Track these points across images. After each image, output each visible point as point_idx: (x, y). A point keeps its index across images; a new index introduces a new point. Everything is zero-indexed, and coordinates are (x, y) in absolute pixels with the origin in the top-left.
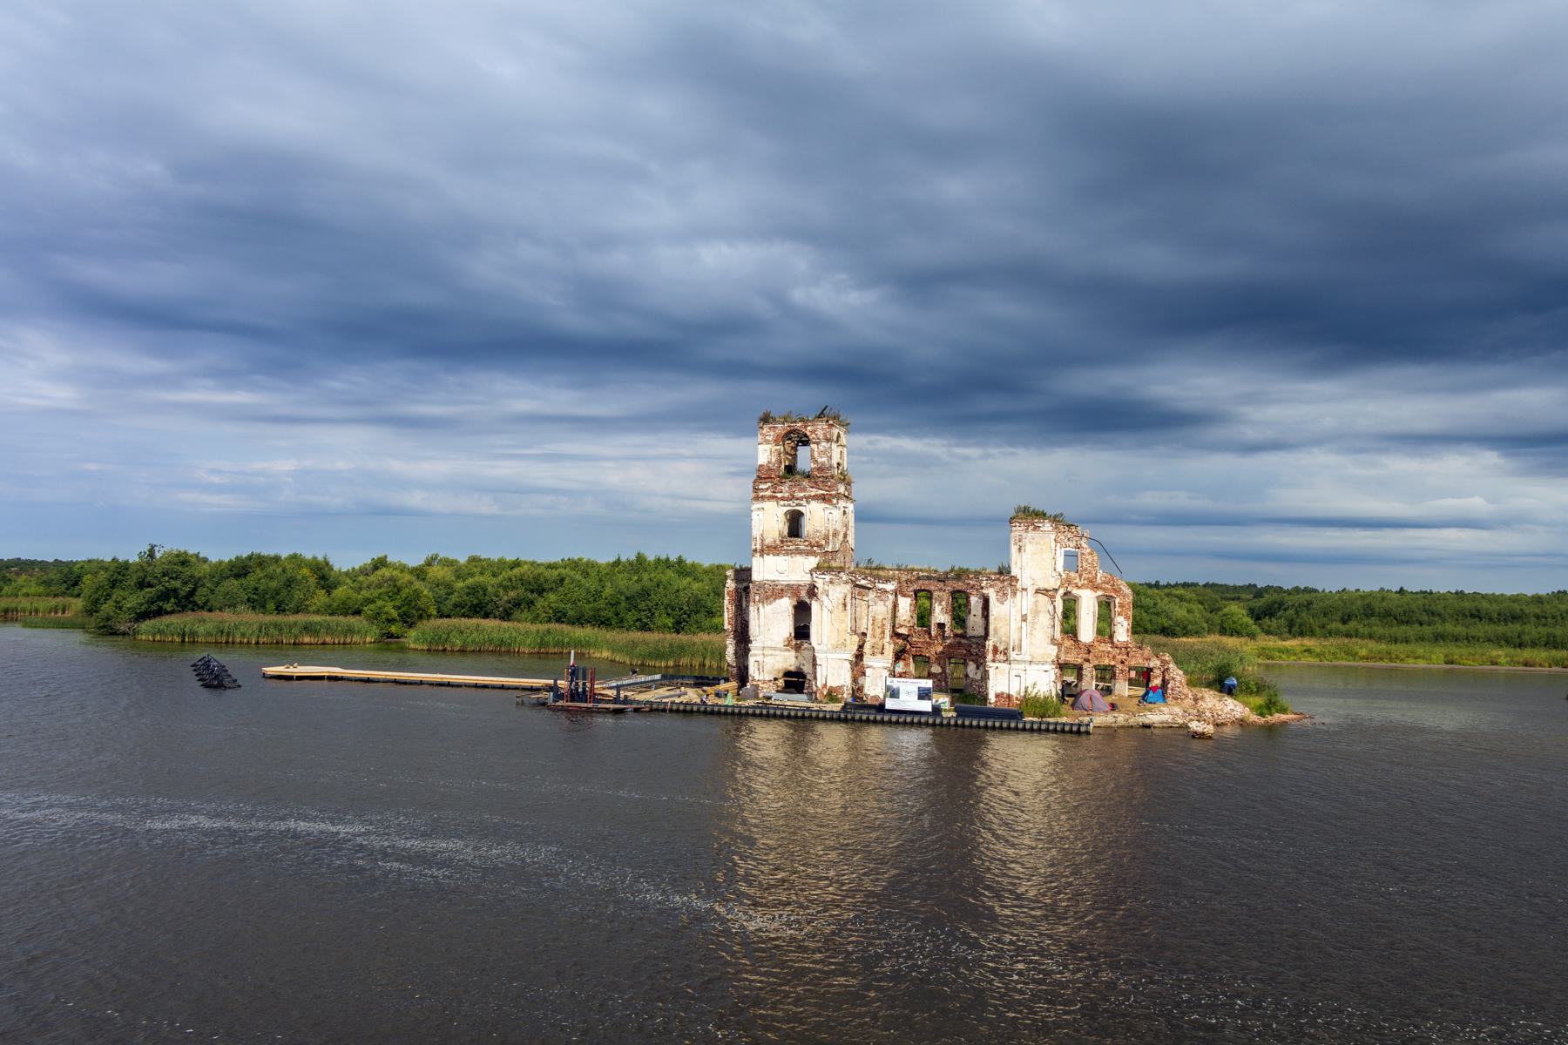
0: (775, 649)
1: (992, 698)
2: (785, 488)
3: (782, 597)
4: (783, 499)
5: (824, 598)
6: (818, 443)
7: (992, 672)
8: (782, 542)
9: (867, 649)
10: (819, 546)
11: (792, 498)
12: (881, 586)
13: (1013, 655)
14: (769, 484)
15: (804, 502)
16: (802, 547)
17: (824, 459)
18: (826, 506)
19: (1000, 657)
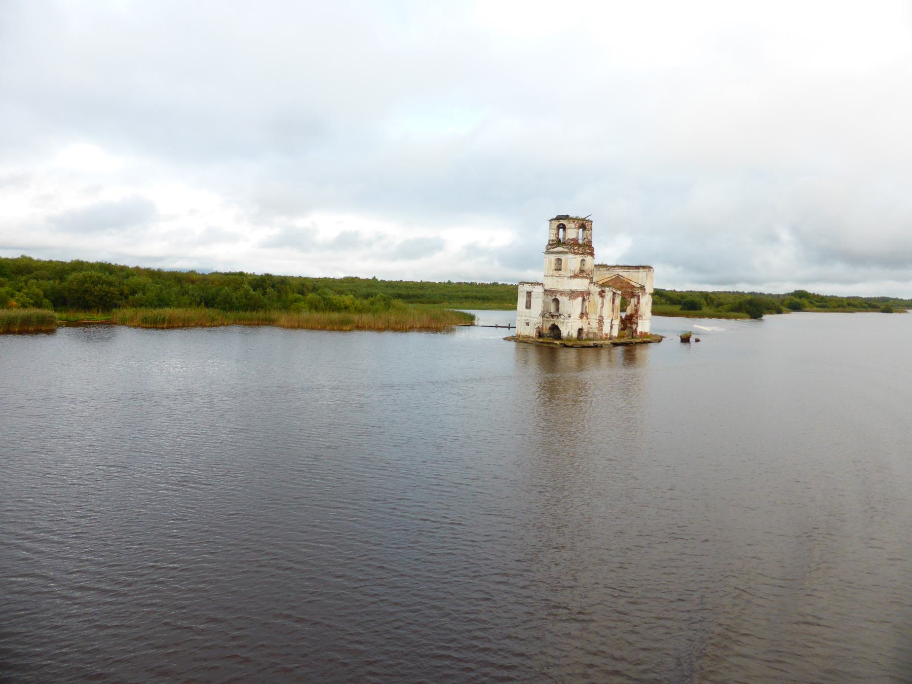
0: (576, 319)
1: (638, 333)
2: (581, 249)
3: (579, 297)
4: (581, 254)
5: (606, 297)
6: (589, 231)
7: (639, 324)
8: (580, 273)
9: (614, 318)
10: (589, 275)
11: (582, 254)
12: (618, 292)
13: (644, 318)
14: (577, 247)
15: (586, 256)
16: (584, 275)
17: (590, 238)
18: (592, 258)
19: (641, 318)
